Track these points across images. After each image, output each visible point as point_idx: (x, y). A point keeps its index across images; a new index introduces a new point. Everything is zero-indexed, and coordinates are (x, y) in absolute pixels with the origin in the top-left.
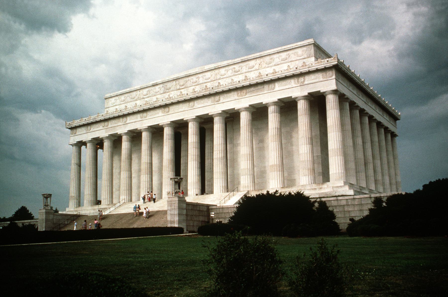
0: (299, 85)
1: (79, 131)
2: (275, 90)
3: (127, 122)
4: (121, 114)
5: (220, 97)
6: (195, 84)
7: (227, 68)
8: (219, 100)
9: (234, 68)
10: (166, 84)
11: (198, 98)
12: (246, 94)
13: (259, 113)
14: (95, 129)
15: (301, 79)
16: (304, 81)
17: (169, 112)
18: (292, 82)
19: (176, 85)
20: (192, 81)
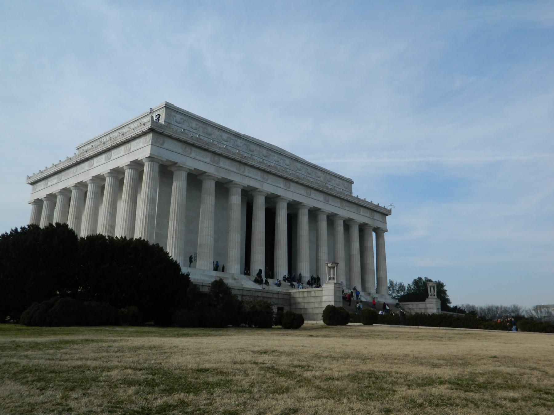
4: (244, 161)
8: (328, 201)
14: (198, 158)
17: (289, 188)
18: (368, 213)
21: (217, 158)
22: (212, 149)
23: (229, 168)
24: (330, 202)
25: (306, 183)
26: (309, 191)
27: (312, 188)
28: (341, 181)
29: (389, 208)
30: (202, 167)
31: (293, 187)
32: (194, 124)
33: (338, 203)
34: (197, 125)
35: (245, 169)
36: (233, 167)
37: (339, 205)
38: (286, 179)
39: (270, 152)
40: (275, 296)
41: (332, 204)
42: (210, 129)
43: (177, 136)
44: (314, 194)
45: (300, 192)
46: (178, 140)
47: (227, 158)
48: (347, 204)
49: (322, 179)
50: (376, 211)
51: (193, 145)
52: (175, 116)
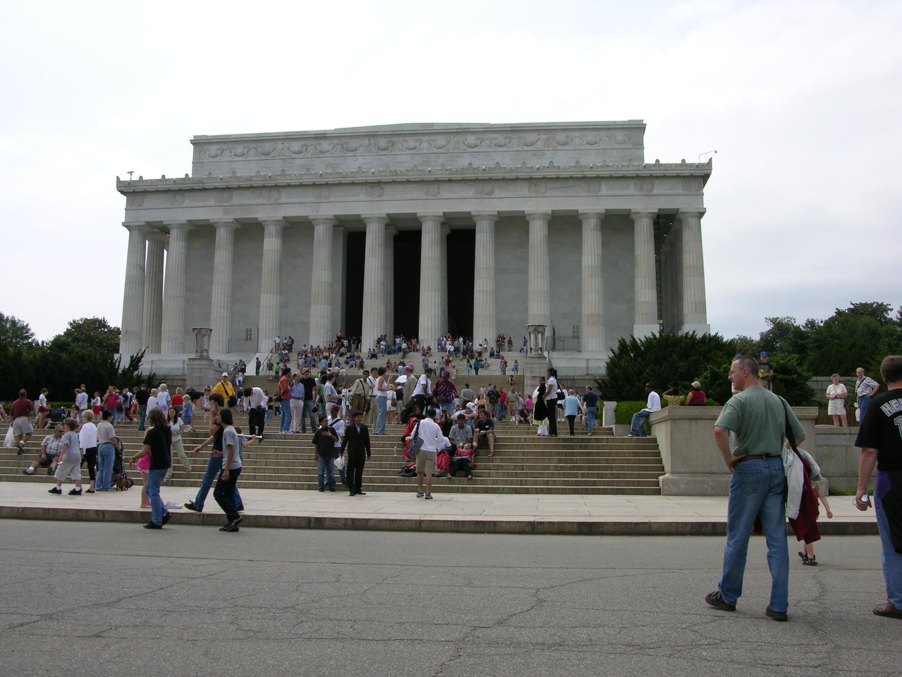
0: (643, 193)
2: (600, 194)
3: (281, 201)
6: (412, 152)
7: (480, 136)
9: (495, 139)
13: (564, 225)
16: (652, 189)
17: (381, 196)
18: (631, 188)
20: (405, 144)
21: (226, 195)
22: (207, 186)
23: (249, 202)
24: (497, 193)
25: (418, 178)
26: (433, 189)
27: (436, 181)
28: (603, 133)
31: (389, 192)
32: (239, 150)
33: (524, 189)
37: (526, 192)
39: (395, 139)
41: (502, 195)
42: (267, 147)
43: (154, 188)
44: (445, 191)
50: (651, 177)
51: (180, 191)
52: (208, 150)
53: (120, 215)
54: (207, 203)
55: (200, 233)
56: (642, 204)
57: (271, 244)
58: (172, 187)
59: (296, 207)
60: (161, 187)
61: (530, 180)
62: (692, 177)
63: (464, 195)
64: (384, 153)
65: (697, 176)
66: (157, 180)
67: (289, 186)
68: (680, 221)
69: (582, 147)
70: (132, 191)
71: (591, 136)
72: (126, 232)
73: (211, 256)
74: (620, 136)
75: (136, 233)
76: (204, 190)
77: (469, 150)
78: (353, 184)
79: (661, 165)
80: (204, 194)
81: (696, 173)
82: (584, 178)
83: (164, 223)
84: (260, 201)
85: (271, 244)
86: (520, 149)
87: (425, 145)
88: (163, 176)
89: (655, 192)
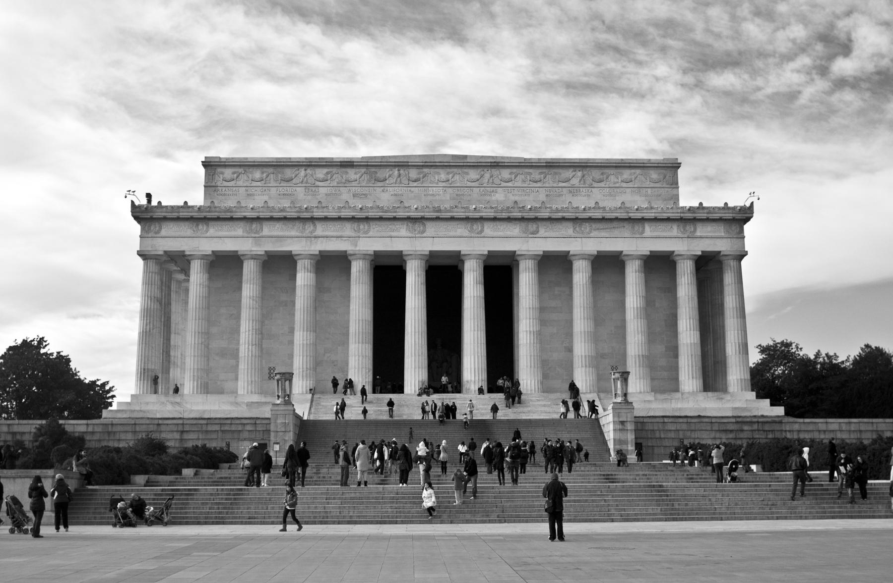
0: (686, 236)
1: (168, 229)
2: (645, 235)
5: (538, 228)
6: (444, 184)
7: (514, 170)
8: (537, 232)
10: (373, 170)
11: (495, 219)
12: (591, 232)
13: (608, 265)
15: (690, 228)
16: (695, 229)
17: (423, 232)
18: (675, 230)
19: (399, 175)
24: (542, 232)
26: (477, 226)
27: (482, 219)
28: (638, 171)
29: (748, 205)
30: (228, 246)
31: (431, 228)
32: (257, 174)
33: (568, 229)
34: (263, 173)
35: (315, 225)
36: (293, 230)
38: (408, 219)
39: (426, 170)
40: (249, 428)
41: (547, 234)
42: (289, 172)
43: (175, 215)
45: (452, 234)
46: (178, 219)
47: (272, 219)
48: (594, 226)
49: (575, 181)
50: (695, 220)
52: (222, 173)
53: (136, 244)
54: (233, 233)
55: (224, 265)
56: (683, 246)
57: (304, 278)
58: (195, 215)
59: (332, 240)
60: (183, 214)
61: (575, 220)
62: (734, 220)
63: (509, 233)
64: (415, 184)
65: (739, 218)
66: (178, 207)
67: (326, 219)
68: (720, 263)
69: (617, 185)
70: (146, 215)
71: (627, 174)
72: (140, 262)
73: (239, 289)
74: (654, 175)
75: (151, 263)
76: (231, 219)
77: (504, 184)
78: (395, 219)
79: (704, 208)
80: (231, 223)
81: (739, 216)
82: (629, 220)
83: (187, 253)
84: (293, 233)
85: (304, 278)
86: (555, 185)
87: (457, 177)
88: (186, 203)
89: (698, 234)
